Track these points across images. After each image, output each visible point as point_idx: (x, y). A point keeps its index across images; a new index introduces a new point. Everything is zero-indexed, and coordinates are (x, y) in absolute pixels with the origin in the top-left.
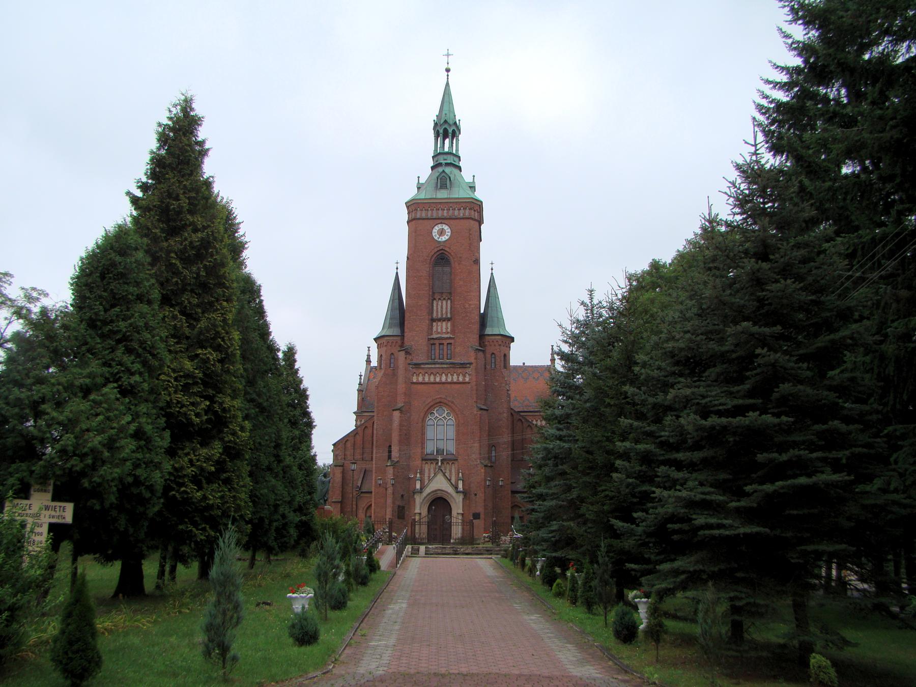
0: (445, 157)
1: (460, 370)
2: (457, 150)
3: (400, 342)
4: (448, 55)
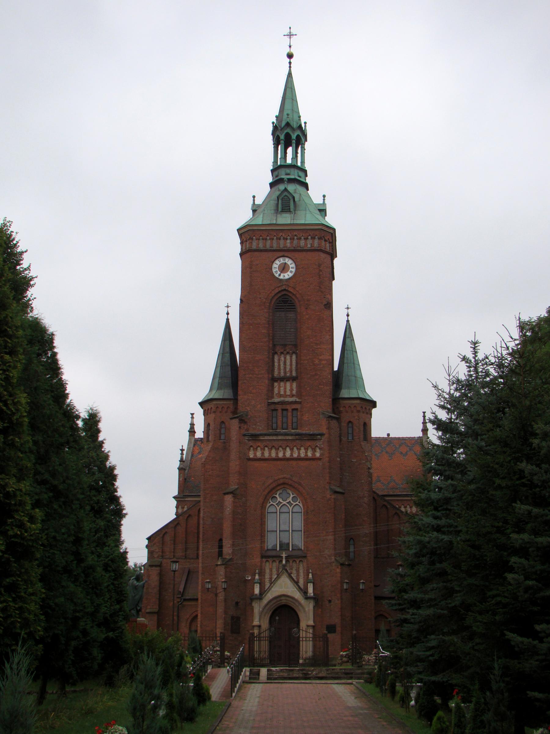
3: (232, 407)
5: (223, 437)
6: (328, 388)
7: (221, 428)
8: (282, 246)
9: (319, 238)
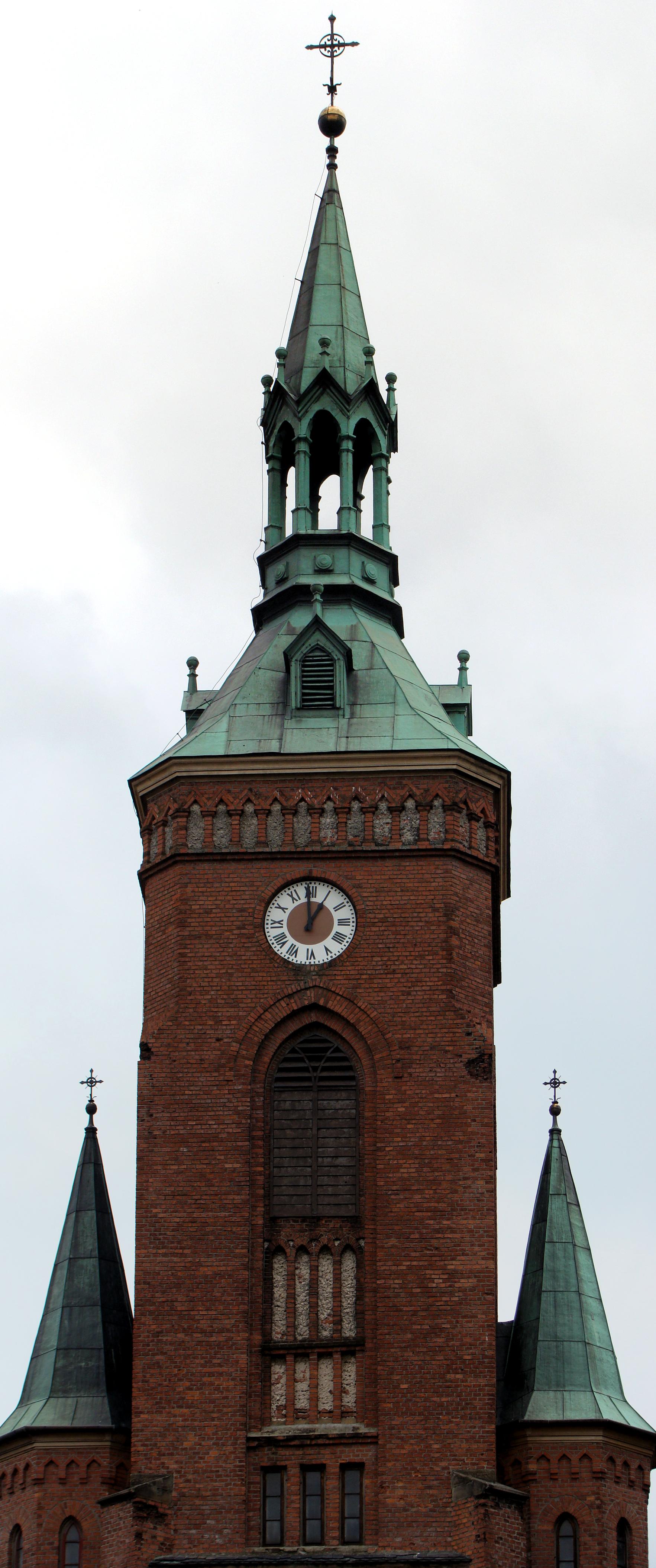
0: (325, 557)
2: (381, 525)
3: (105, 1461)
4: (332, 46)
6: (482, 1381)
7: (64, 1542)
8: (302, 840)
9: (446, 808)
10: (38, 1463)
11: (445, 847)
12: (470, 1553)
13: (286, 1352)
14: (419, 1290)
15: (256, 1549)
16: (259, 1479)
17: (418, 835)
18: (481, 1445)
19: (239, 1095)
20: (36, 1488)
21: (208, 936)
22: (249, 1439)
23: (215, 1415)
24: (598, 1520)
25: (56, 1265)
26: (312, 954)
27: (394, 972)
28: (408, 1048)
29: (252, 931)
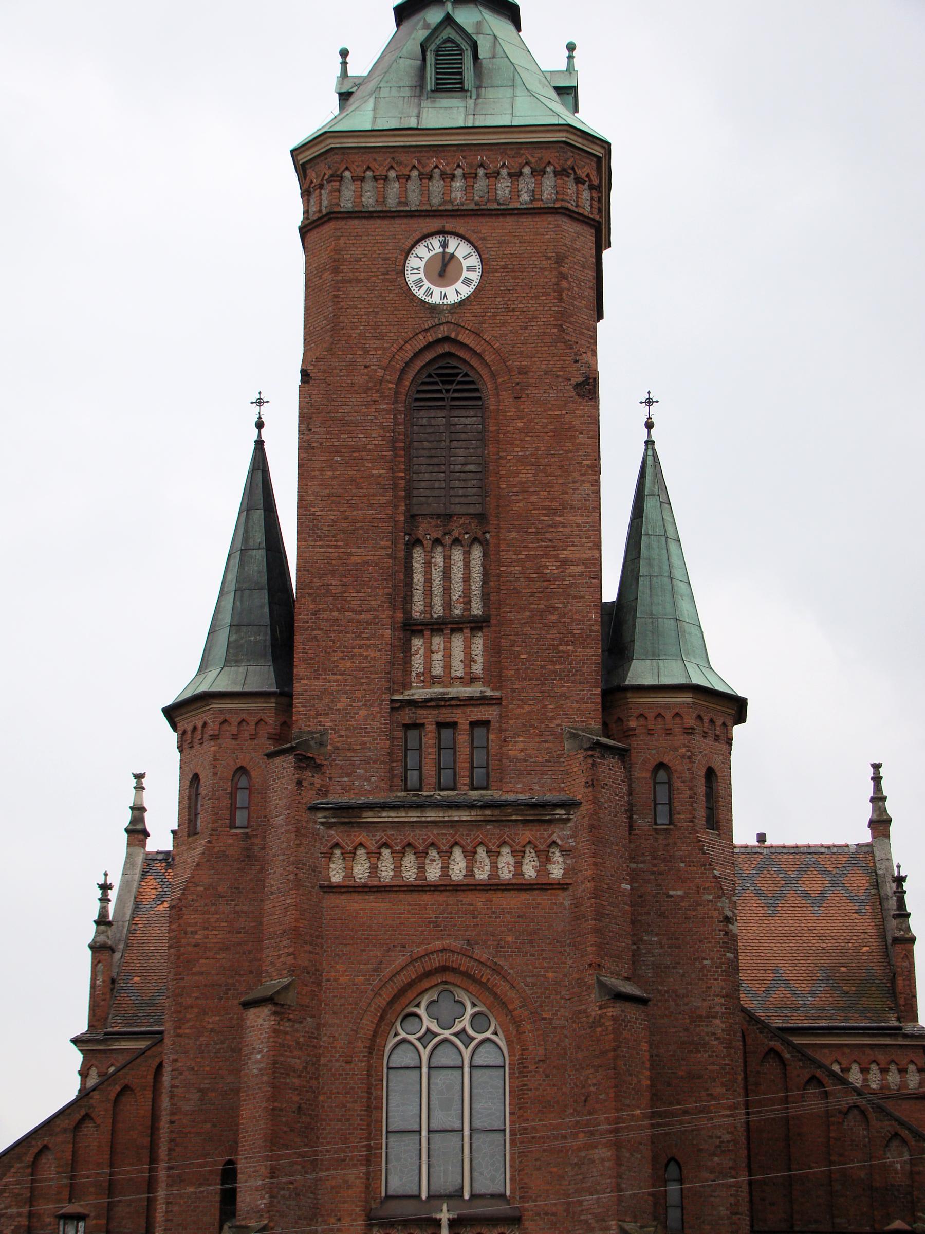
1: (526, 834)
3: (271, 720)
5: (241, 817)
6: (589, 652)
7: (235, 789)
8: (436, 200)
9: (556, 173)
10: (213, 722)
11: (556, 206)
12: (580, 796)
13: (423, 628)
14: (535, 576)
15: (399, 794)
16: (400, 734)
17: (533, 196)
18: (589, 706)
19: (384, 413)
20: (212, 743)
21: (359, 281)
22: (392, 701)
23: (363, 681)
24: (689, 769)
25: (229, 556)
26: (445, 295)
27: (513, 310)
28: (526, 373)
29: (394, 277)
